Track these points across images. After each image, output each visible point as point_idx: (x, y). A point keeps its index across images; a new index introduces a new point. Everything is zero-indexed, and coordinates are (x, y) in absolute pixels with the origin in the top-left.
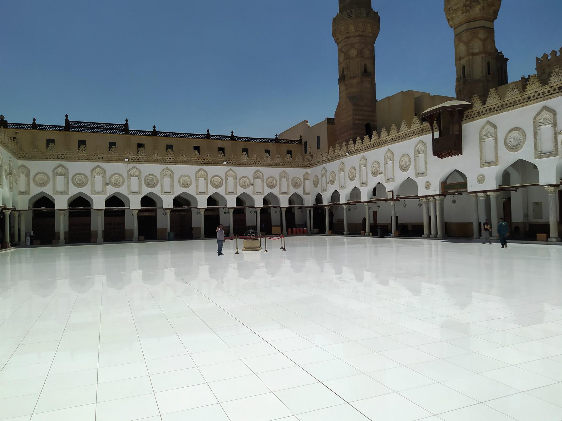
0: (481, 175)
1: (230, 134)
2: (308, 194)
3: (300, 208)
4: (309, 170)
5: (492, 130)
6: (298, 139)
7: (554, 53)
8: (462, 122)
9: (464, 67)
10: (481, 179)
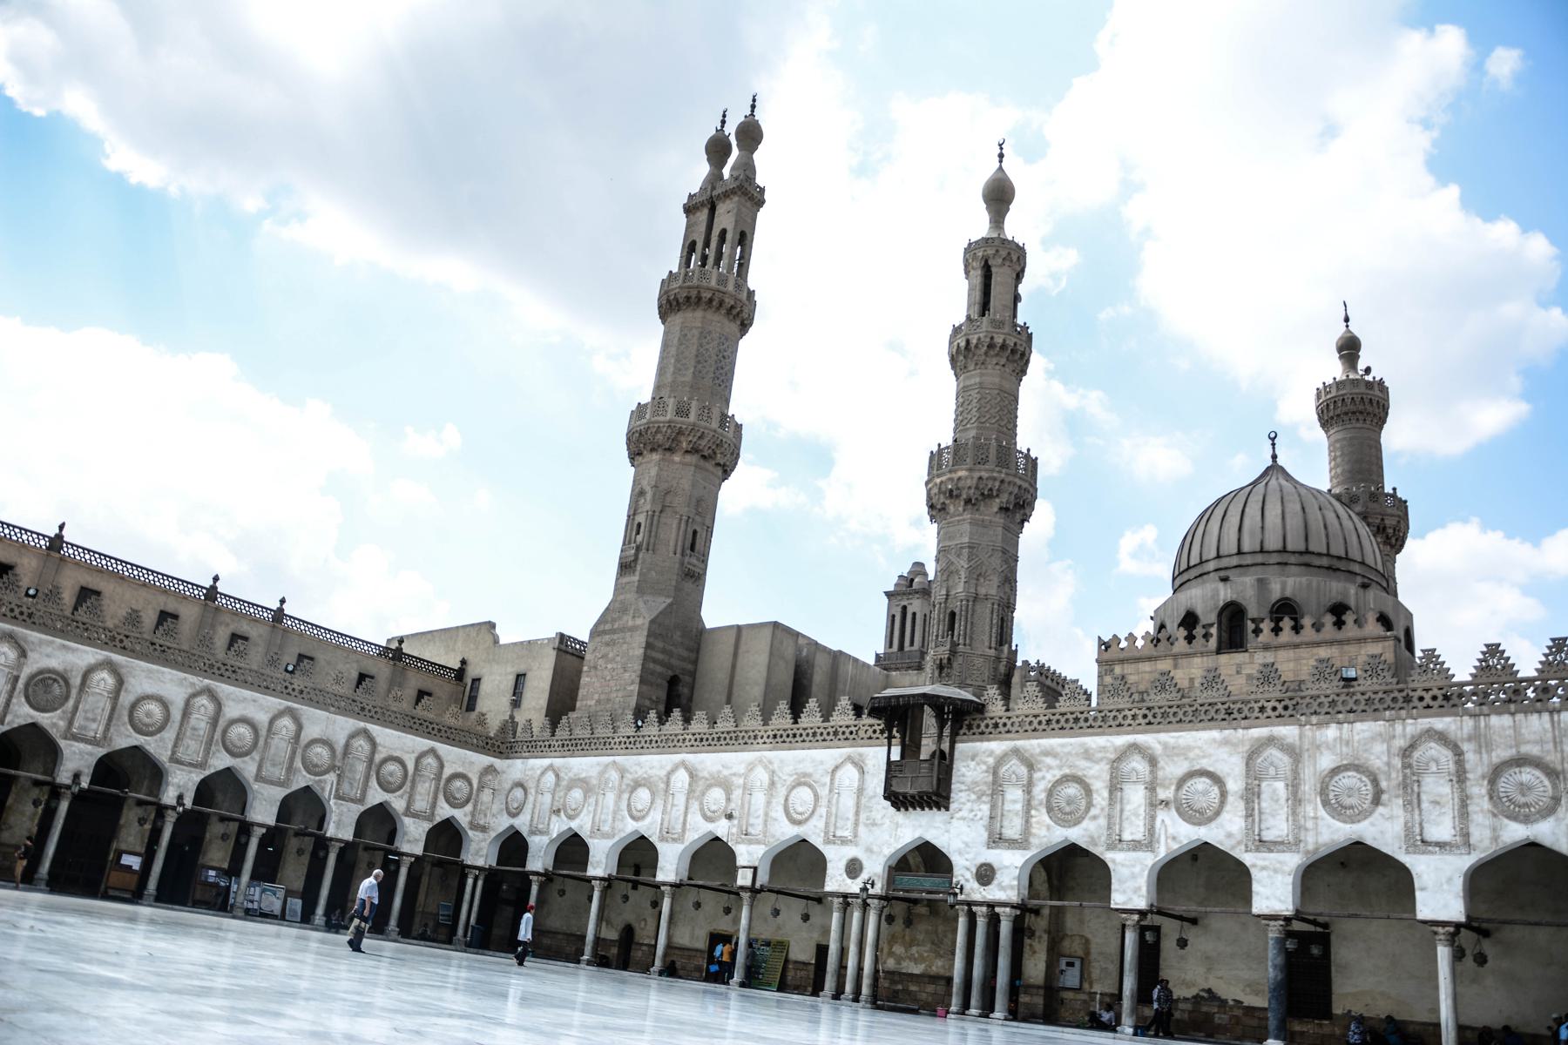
0: (982, 865)
1: (275, 605)
4: (498, 763)
5: (1023, 770)
6: (457, 666)
9: (953, 615)
10: (985, 874)
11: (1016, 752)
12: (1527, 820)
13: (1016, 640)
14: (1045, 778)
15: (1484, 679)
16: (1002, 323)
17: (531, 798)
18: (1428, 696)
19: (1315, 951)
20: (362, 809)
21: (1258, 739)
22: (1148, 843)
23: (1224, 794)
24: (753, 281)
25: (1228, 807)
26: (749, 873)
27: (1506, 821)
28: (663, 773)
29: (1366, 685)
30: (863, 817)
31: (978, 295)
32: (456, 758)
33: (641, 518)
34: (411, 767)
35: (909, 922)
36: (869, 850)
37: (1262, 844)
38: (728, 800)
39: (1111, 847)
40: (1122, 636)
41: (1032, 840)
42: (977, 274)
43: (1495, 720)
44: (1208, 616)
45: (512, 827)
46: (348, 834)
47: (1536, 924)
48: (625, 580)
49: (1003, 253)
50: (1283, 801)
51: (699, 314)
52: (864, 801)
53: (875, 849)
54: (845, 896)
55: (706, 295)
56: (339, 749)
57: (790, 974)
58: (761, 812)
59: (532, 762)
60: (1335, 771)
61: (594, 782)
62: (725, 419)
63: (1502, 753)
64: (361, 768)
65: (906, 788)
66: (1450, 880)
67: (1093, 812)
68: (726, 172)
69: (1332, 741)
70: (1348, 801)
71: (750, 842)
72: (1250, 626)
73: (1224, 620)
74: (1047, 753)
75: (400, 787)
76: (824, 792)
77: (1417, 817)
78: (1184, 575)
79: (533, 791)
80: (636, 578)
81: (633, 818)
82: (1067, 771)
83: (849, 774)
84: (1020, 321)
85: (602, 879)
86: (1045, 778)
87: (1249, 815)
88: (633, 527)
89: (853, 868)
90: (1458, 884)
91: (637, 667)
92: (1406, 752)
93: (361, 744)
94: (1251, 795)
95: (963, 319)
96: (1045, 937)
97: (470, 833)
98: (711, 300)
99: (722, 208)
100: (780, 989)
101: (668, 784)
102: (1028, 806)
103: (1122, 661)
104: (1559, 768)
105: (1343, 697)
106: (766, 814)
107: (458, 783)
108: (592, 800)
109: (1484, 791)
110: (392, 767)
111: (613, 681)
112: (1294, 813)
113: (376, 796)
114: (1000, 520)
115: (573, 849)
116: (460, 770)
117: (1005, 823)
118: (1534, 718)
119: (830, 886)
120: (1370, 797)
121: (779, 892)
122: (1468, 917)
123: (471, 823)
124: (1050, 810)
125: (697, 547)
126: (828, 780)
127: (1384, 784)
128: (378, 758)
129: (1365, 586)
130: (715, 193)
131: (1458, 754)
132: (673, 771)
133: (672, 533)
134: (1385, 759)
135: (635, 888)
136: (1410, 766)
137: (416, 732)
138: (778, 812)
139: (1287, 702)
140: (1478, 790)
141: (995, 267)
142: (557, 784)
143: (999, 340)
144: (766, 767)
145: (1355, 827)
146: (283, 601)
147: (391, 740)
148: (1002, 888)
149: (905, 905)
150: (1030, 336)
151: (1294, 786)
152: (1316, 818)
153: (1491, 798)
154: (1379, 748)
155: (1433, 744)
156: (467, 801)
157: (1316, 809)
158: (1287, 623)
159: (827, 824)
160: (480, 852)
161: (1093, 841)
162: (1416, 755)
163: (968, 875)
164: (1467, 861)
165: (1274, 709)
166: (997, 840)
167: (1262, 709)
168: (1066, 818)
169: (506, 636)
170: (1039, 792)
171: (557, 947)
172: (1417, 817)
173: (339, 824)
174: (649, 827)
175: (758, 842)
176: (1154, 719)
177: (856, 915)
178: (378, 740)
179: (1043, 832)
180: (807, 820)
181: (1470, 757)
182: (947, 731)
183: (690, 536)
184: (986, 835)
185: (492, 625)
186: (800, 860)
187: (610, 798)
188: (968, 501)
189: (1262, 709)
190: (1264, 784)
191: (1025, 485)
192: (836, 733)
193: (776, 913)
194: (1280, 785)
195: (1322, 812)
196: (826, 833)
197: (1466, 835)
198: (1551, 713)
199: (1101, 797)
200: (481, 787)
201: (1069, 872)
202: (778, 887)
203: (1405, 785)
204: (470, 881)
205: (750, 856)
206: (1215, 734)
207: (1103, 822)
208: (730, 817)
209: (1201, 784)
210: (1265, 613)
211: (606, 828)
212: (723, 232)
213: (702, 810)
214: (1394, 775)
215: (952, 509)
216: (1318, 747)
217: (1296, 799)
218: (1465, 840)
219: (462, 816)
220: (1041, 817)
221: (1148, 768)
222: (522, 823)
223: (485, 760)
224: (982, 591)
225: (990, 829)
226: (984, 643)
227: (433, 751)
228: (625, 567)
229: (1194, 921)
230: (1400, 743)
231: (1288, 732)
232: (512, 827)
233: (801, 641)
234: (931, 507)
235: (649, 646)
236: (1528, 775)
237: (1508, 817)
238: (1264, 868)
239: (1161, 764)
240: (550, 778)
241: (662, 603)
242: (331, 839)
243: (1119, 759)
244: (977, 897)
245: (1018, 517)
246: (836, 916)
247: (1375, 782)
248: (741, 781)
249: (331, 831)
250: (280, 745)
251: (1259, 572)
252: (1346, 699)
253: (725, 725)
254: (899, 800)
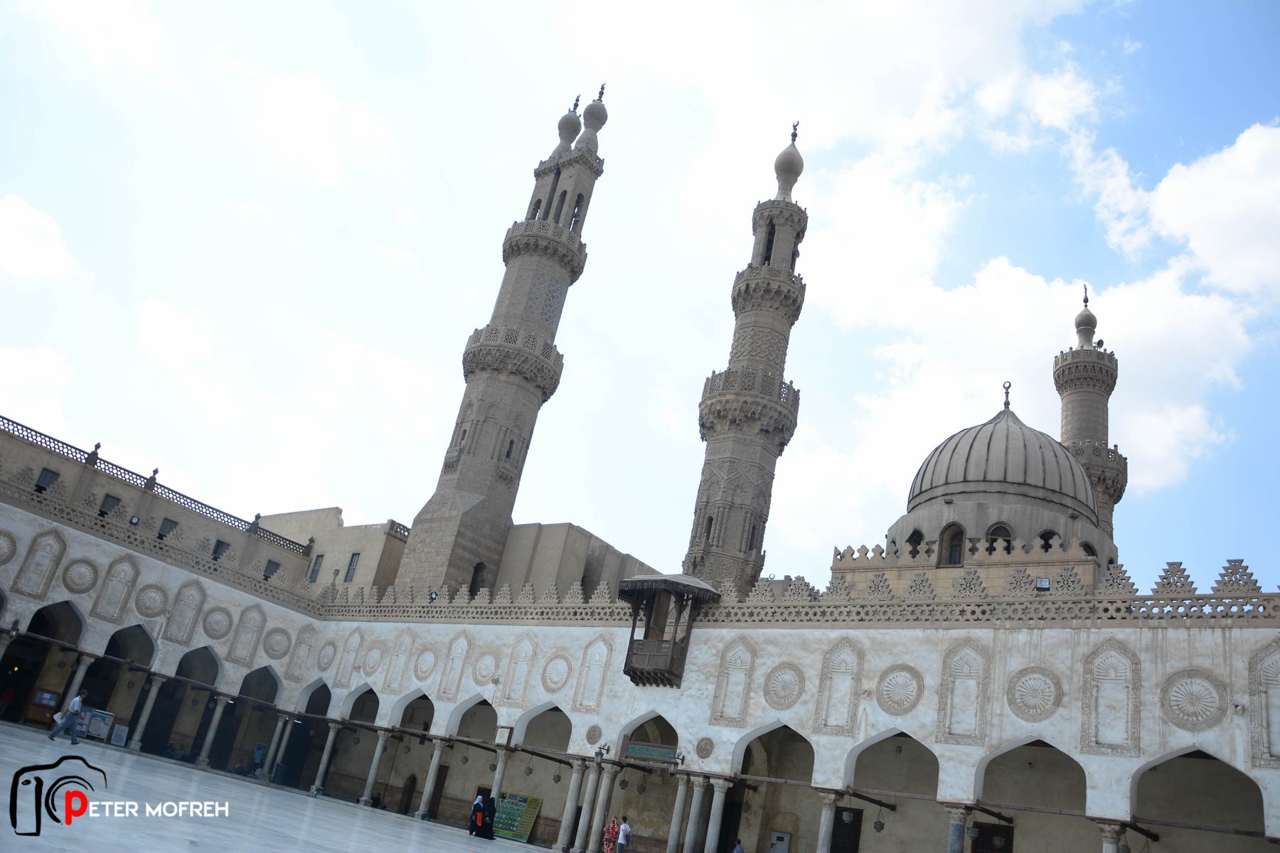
1: (148, 475)
2: (297, 680)
3: (260, 708)
4: (316, 623)
5: (747, 656)
6: (305, 543)
7: (864, 550)
8: (695, 624)
9: (711, 519)
10: (705, 748)
11: (743, 639)
12: (1194, 728)
13: (766, 546)
14: (766, 664)
15: (1165, 595)
16: (779, 272)
17: (339, 656)
18: (1112, 608)
19: (998, 842)
20: (187, 650)
21: (956, 640)
22: (849, 730)
23: (921, 688)
24: (587, 236)
25: (923, 701)
26: (507, 732)
27: (1175, 728)
28: (447, 640)
29: (1057, 595)
30: (606, 689)
31: (762, 248)
32: (279, 615)
33: (467, 426)
34: (236, 619)
35: (642, 789)
36: (609, 719)
37: (951, 737)
38: (497, 667)
39: (816, 730)
40: (856, 548)
42: (763, 231)
43: (1171, 633)
44: (931, 534)
45: (320, 679)
46: (171, 671)
47: (1197, 828)
48: (449, 477)
49: (787, 214)
50: (973, 698)
51: (535, 258)
52: (609, 674)
54: (584, 759)
55: (543, 243)
56: (172, 596)
57: (540, 829)
58: (523, 680)
59: (344, 624)
60: (1023, 673)
61: (391, 644)
62: (549, 349)
63: (1175, 665)
64: (190, 614)
65: (643, 665)
66: (1119, 781)
67: (805, 697)
68: (573, 146)
69: (1022, 645)
70: (1032, 701)
71: (511, 706)
72: (968, 545)
73: (946, 537)
74: (769, 641)
75: (224, 635)
76: (576, 665)
77: (1093, 720)
78: (918, 497)
79: (341, 649)
80: (456, 476)
81: (418, 677)
82: (785, 659)
83: (601, 648)
84: (796, 273)
85: (386, 730)
86: (766, 664)
87: (942, 709)
88: (460, 432)
89: (594, 734)
90: (1126, 785)
91: (448, 552)
92: (1089, 659)
93: (192, 593)
94: (945, 690)
95: (745, 267)
96: (760, 812)
97: (285, 682)
98: (546, 248)
99: (564, 174)
100: (530, 841)
101: (450, 649)
102: (748, 688)
103: (853, 570)
104: (1227, 680)
105: (1036, 605)
106: (527, 682)
107: (278, 637)
108: (388, 660)
109: (1156, 699)
110: (218, 617)
111: (427, 566)
112: (983, 710)
113: (200, 641)
114: (760, 440)
115: (367, 702)
116: (281, 626)
117: (727, 703)
118: (1207, 634)
119: (573, 749)
120: (1052, 698)
121: (533, 753)
122: (1133, 817)
123: (286, 673)
124: (766, 693)
125: (513, 455)
126: (581, 654)
127: (1065, 688)
128: (206, 607)
129: (1074, 517)
130: (561, 161)
131: (1136, 663)
132: (455, 639)
133: (491, 441)
134: (1069, 664)
135: (422, 743)
136: (1091, 672)
137: (244, 588)
138: (537, 681)
139: (985, 607)
140: (1151, 697)
141: (780, 227)
142: (361, 645)
143: (774, 286)
144: (531, 640)
145: (1037, 726)
146: (156, 472)
147: (220, 592)
148: (718, 762)
149: (640, 773)
150: (803, 287)
151: (984, 685)
152: (1001, 715)
153: (1163, 705)
154: (1064, 653)
155: (1113, 653)
156: (285, 653)
157: (1002, 707)
158: (1000, 544)
159: (576, 695)
160: (292, 700)
161: (802, 724)
162: (1097, 661)
163: (691, 748)
164: (1135, 764)
165: (973, 613)
166: (718, 717)
167: (962, 612)
168: (779, 700)
169: (349, 520)
170: (759, 677)
171: (340, 788)
172: (1093, 720)
173: (163, 662)
174: (429, 687)
175: (517, 706)
176: (864, 616)
177: (592, 777)
178: (209, 592)
179: (759, 713)
180: (559, 689)
181: (1147, 666)
182: (686, 614)
183: (507, 445)
184: (709, 712)
185: (338, 511)
186: (551, 723)
187: (403, 658)
188: (733, 422)
189: (962, 612)
190: (957, 682)
191: (785, 412)
192: (592, 613)
193: (530, 771)
194: (972, 683)
195: (1007, 710)
196: (574, 702)
197: (1136, 739)
198: (1223, 629)
199: (812, 685)
200: (299, 643)
201: (782, 749)
202: (529, 748)
203: (1085, 689)
204: (280, 724)
205: (508, 716)
206: (918, 633)
207: (811, 707)
208: (496, 682)
209: (902, 677)
210: (981, 534)
211: (395, 686)
212: (565, 193)
213: (474, 674)
214: (1075, 679)
215: (718, 428)
216: (1009, 650)
217: (985, 696)
218: (1135, 744)
219: (278, 667)
220: (758, 699)
221: (856, 660)
222: (328, 678)
223: (305, 619)
224: (738, 501)
225: (713, 707)
226: (734, 548)
227: (258, 607)
228: (449, 466)
229: (893, 808)
230: (1083, 650)
231: (983, 634)
232: (320, 679)
233: (593, 542)
234: (702, 425)
235: (459, 534)
236: (1198, 686)
237: (1177, 725)
238: (951, 759)
239: (869, 657)
240: (356, 639)
241: (474, 499)
242: (155, 674)
243: (831, 651)
244: (695, 768)
245: (777, 440)
246: (575, 777)
247: (1058, 685)
248: (510, 651)
249: (156, 667)
250: (117, 588)
251: (981, 498)
252: (1039, 609)
253: (501, 601)
254: (638, 676)
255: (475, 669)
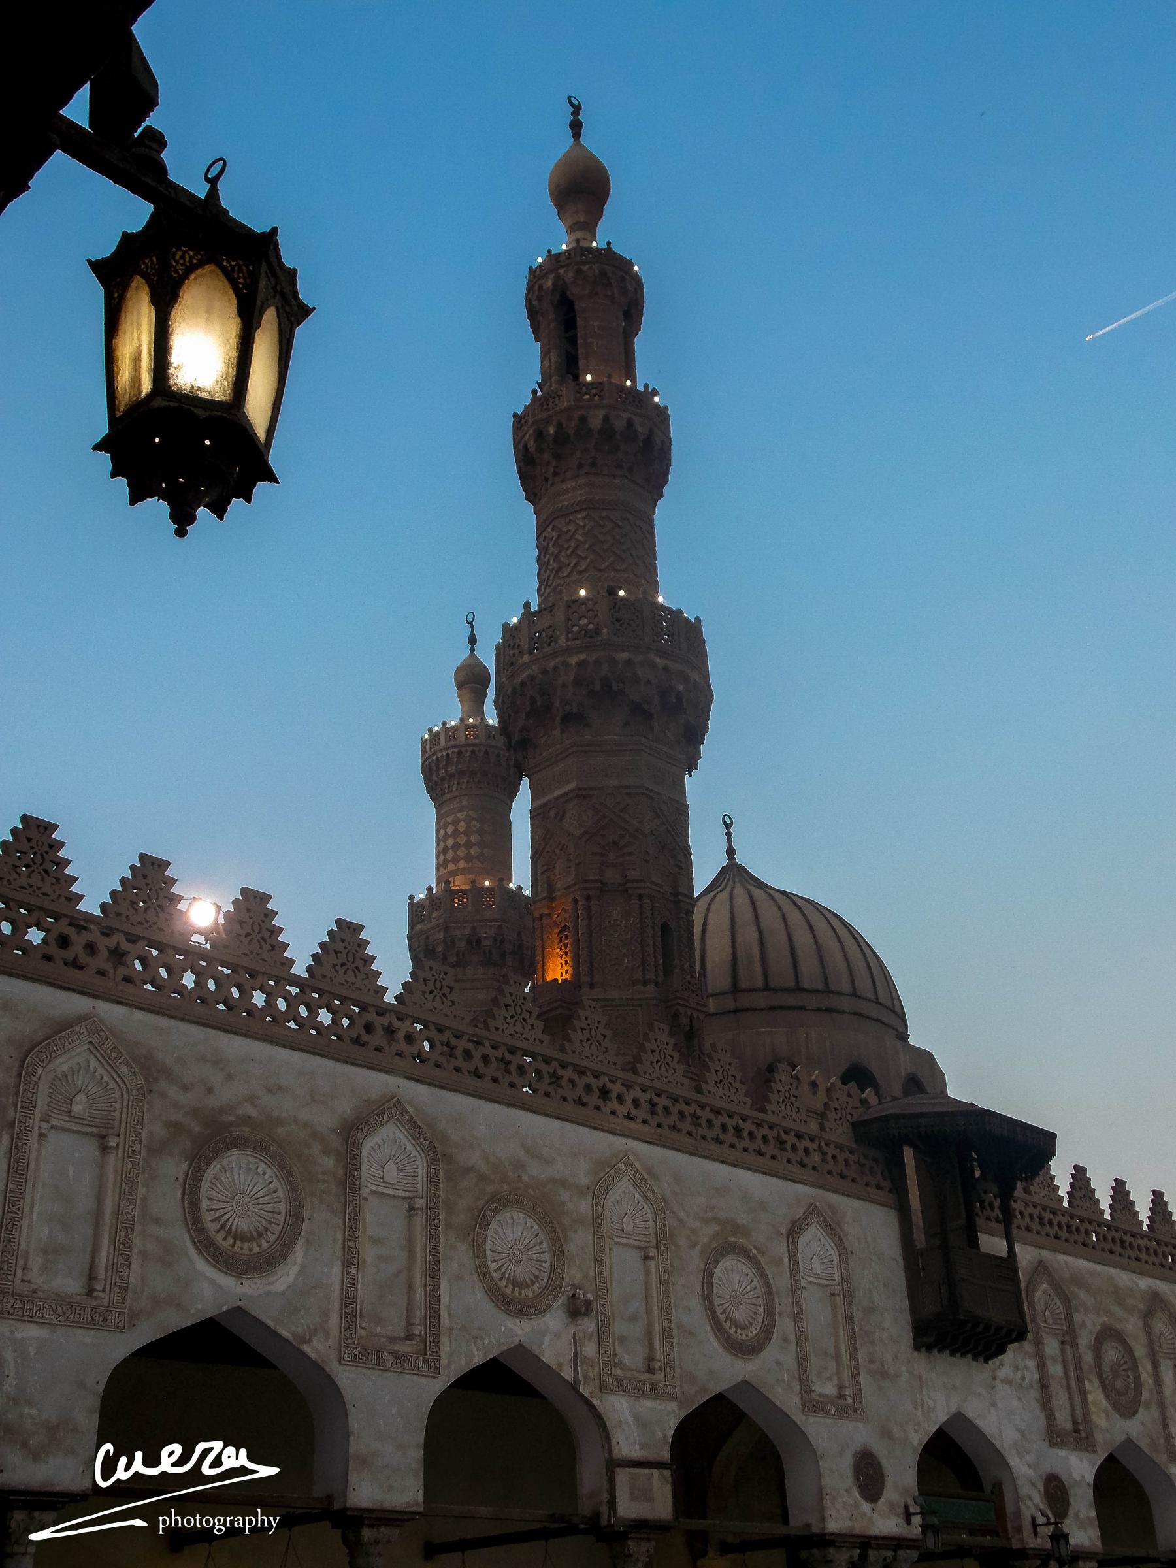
14: (1089, 1324)
41: (1099, 1438)
53: (896, 1431)
67: (1146, 1395)
74: (1079, 1281)
86: (1089, 1324)
119: (835, 1524)
126: (782, 1250)
138: (690, 1313)
166: (1055, 1437)
207: (1155, 1412)
255: (478, 1250)
